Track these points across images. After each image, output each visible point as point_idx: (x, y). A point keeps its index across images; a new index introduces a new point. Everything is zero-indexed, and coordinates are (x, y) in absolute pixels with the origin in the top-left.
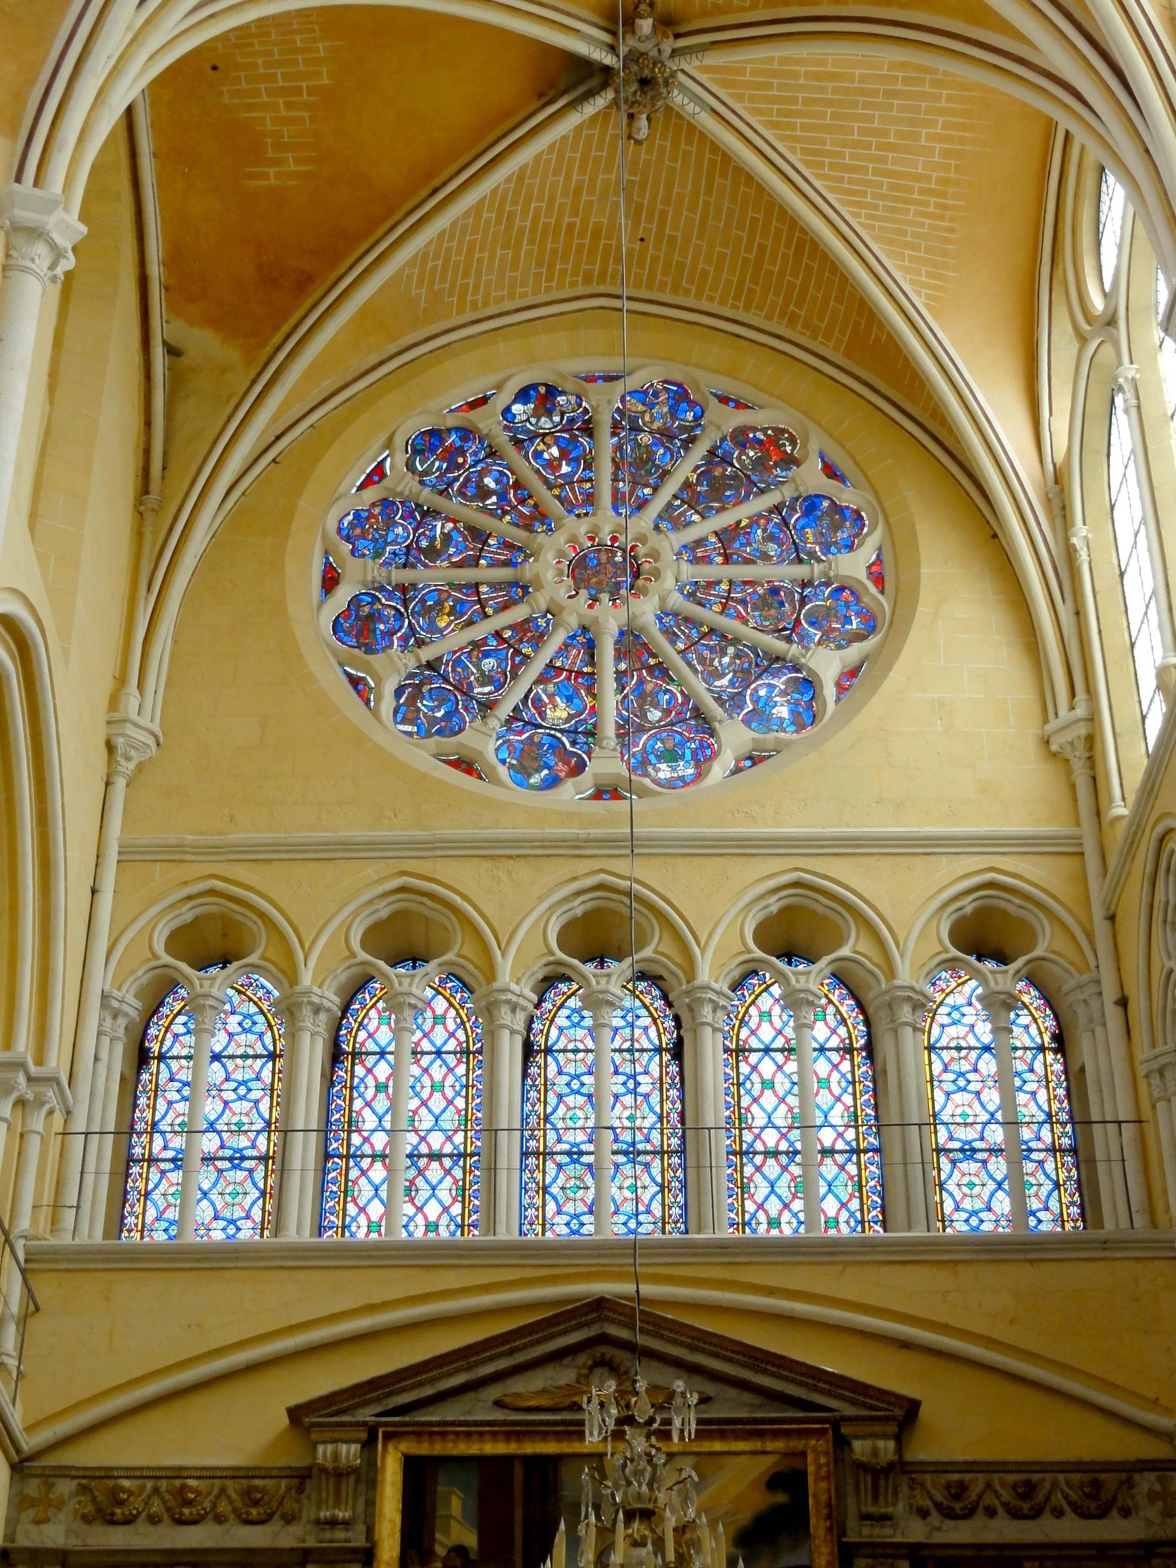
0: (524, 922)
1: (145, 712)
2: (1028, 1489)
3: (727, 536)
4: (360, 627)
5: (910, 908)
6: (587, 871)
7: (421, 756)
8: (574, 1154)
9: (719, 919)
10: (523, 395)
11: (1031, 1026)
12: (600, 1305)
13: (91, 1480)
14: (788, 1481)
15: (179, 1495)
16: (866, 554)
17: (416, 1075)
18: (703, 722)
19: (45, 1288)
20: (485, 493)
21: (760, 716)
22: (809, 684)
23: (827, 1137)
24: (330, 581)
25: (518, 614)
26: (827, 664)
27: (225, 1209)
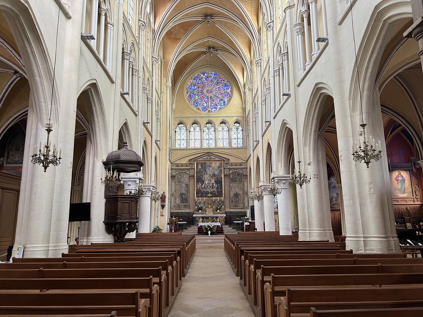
0: (203, 122)
1: (174, 106)
2: (236, 165)
3: (219, 88)
4: (190, 96)
5: (231, 121)
6: (208, 119)
7: (195, 109)
8: (207, 139)
9: (217, 122)
10: (202, 74)
11: (240, 128)
12: (209, 152)
13: (176, 164)
14: (221, 164)
15: (182, 165)
16: (230, 89)
17: (195, 133)
18: (217, 105)
19: (172, 151)
20: (199, 84)
21: (221, 105)
22: (224, 102)
23: (225, 138)
24: (187, 92)
25: (202, 96)
26: (226, 100)
27: (184, 145)
